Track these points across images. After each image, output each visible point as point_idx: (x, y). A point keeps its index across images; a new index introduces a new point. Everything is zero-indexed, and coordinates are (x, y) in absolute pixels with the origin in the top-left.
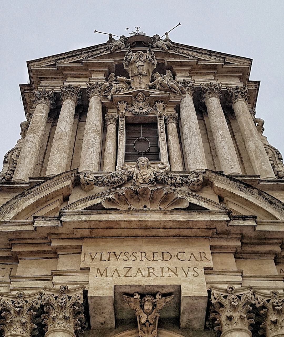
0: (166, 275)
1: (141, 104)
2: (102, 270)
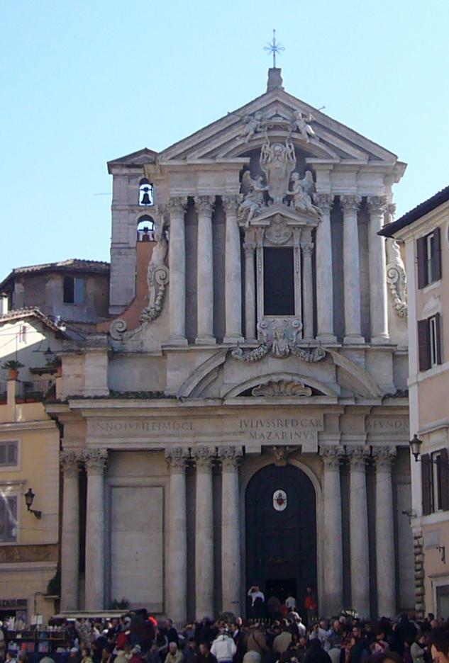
0: (293, 437)
1: (278, 227)
2: (253, 434)
